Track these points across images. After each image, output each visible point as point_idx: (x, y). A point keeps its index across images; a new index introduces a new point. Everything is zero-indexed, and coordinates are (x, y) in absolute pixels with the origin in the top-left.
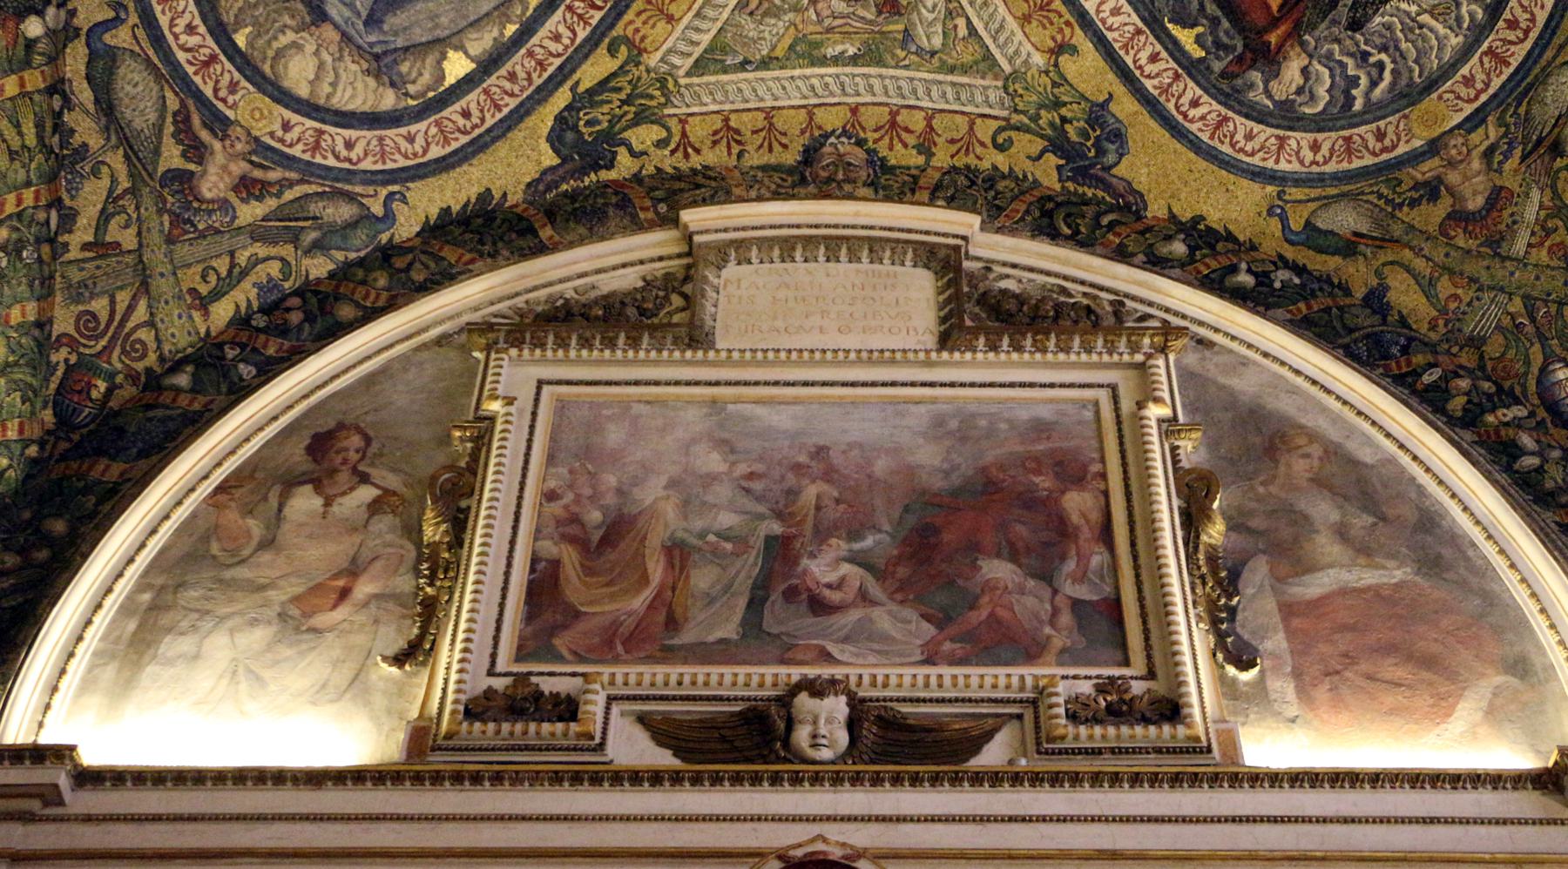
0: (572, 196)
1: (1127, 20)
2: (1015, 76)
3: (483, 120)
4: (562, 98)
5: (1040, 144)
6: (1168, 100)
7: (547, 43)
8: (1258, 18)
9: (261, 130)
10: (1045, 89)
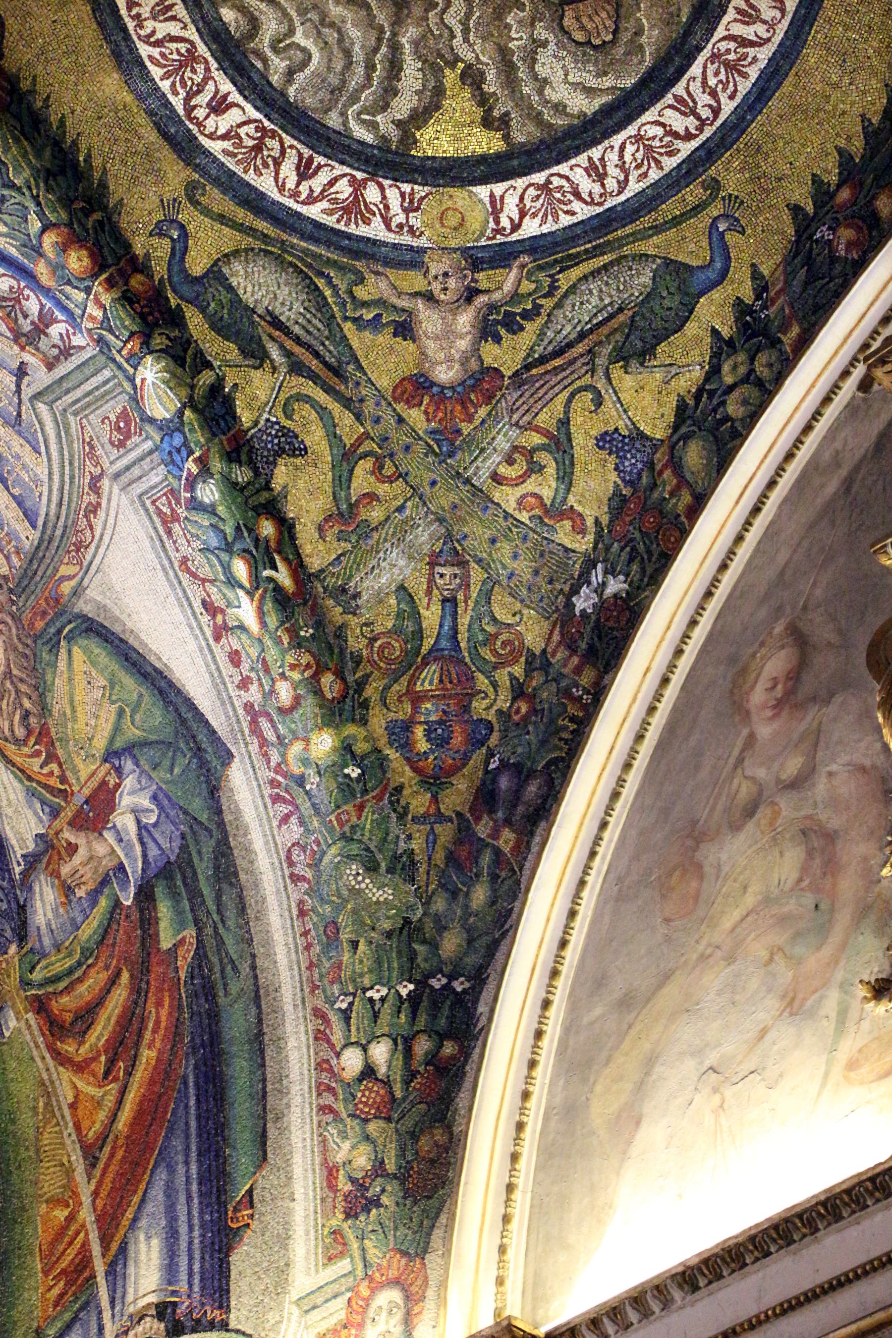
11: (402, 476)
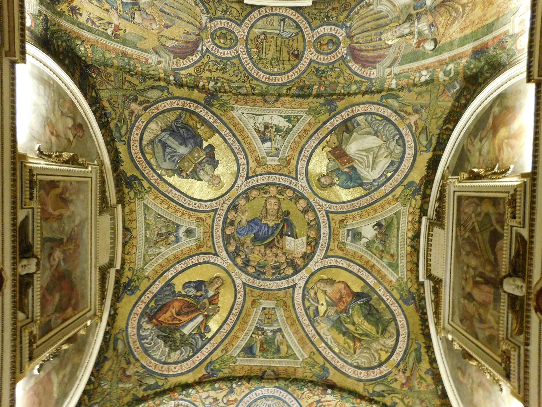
0: (121, 180)
4: (140, 177)
8: (157, 317)
9: (143, 117)
11: (409, 397)
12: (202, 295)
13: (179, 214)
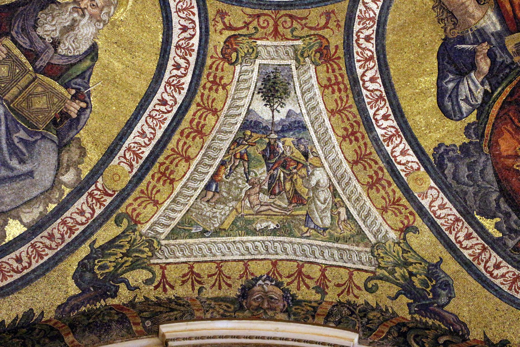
0: (88, 315)
1: (450, 212)
2: (377, 245)
3: (30, 264)
4: (84, 251)
5: (395, 289)
6: (480, 264)
7: (75, 216)
10: (398, 254)
12: (491, 54)
13: (211, 119)
